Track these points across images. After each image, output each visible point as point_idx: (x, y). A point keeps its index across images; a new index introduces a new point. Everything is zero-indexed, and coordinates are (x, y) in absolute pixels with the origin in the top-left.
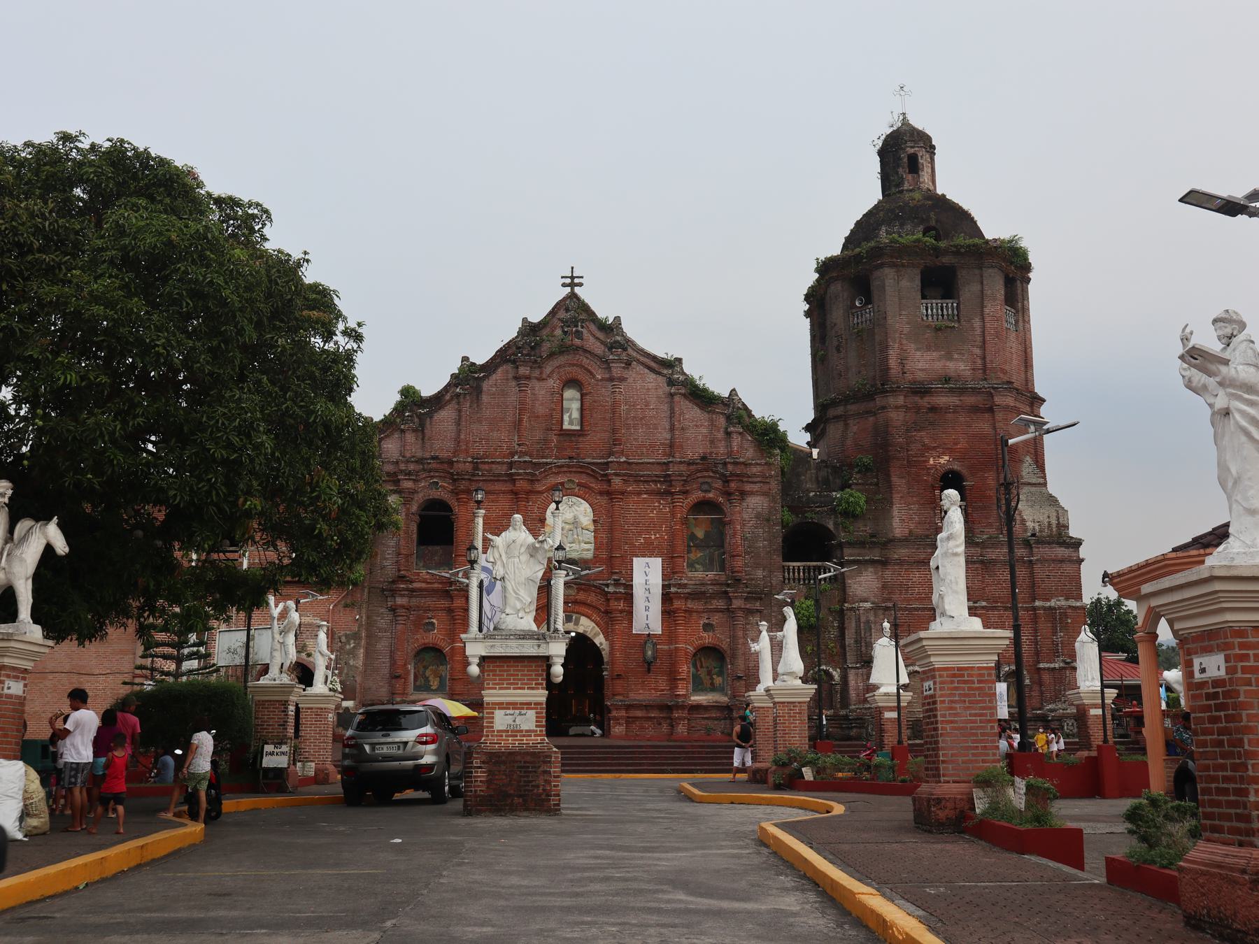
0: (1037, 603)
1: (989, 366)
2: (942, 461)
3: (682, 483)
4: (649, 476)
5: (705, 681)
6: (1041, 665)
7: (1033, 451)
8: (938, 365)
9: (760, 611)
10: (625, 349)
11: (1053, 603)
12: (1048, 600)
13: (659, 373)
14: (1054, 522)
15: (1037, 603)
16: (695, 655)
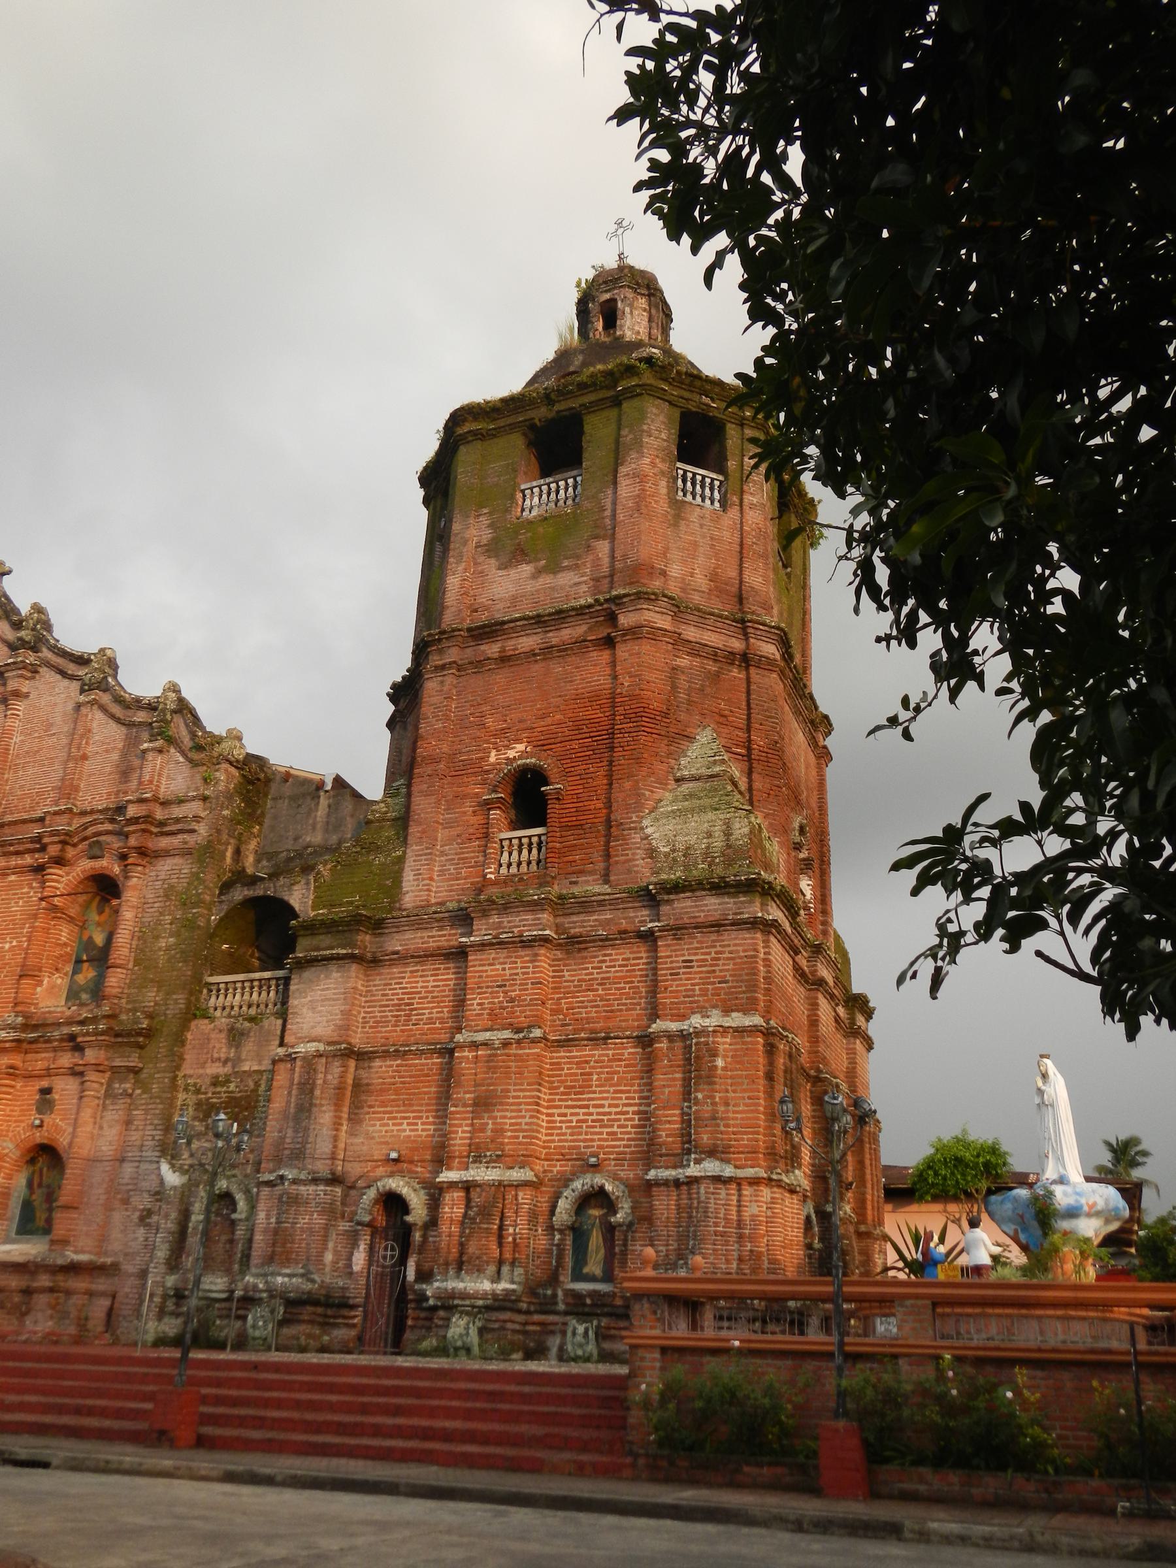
0: (658, 1026)
1: (618, 565)
2: (511, 754)
3: (59, 846)
4: (20, 842)
5: (38, 1214)
6: (652, 1174)
7: (740, 718)
8: (531, 586)
9: (136, 1071)
10: (35, 649)
11: (696, 1021)
12: (683, 1017)
13: (72, 678)
14: (718, 843)
15: (658, 1026)
16: (32, 1161)
